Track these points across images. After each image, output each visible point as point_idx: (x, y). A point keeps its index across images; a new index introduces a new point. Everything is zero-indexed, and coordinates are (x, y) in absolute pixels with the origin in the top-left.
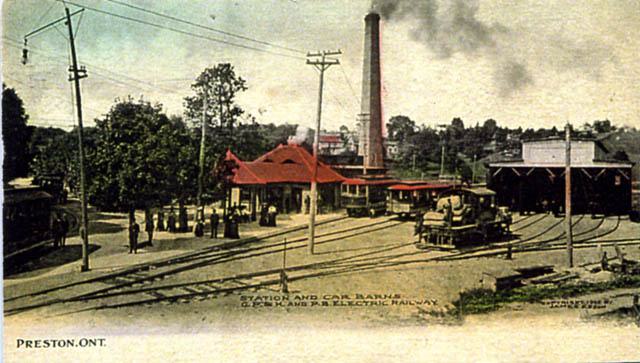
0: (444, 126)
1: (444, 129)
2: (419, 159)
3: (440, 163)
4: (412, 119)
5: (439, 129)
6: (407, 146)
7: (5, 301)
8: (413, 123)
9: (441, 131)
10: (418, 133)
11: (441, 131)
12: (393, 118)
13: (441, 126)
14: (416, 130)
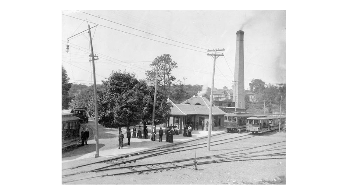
0: (282, 84)
1: (281, 86)
2: (267, 103)
3: (280, 105)
4: (263, 81)
5: (279, 86)
6: (261, 95)
7: (237, 41)
8: (264, 83)
9: (280, 87)
10: (267, 88)
11: (280, 87)
12: (253, 80)
13: (280, 85)
14: (266, 86)
